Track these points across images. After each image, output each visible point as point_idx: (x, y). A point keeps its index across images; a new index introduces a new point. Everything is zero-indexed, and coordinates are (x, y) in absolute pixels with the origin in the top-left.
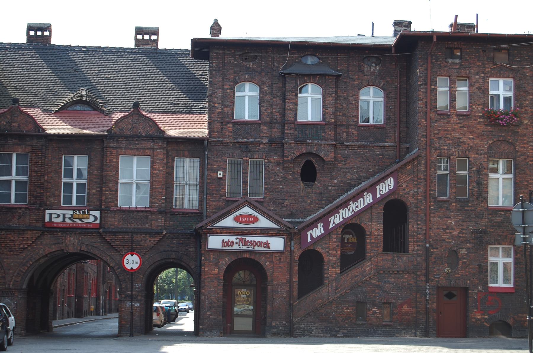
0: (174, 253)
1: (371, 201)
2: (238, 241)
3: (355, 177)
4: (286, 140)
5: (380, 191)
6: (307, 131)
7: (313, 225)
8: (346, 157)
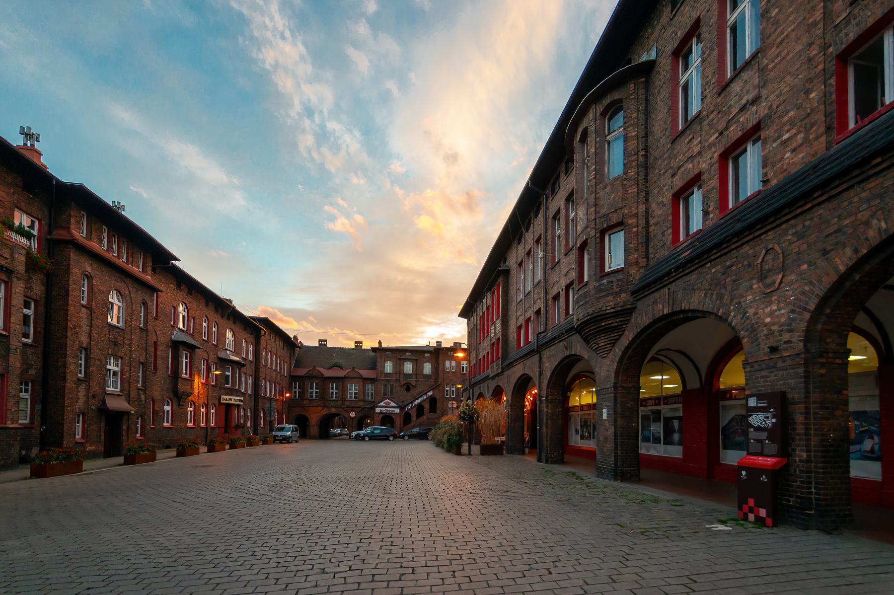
7: (408, 405)
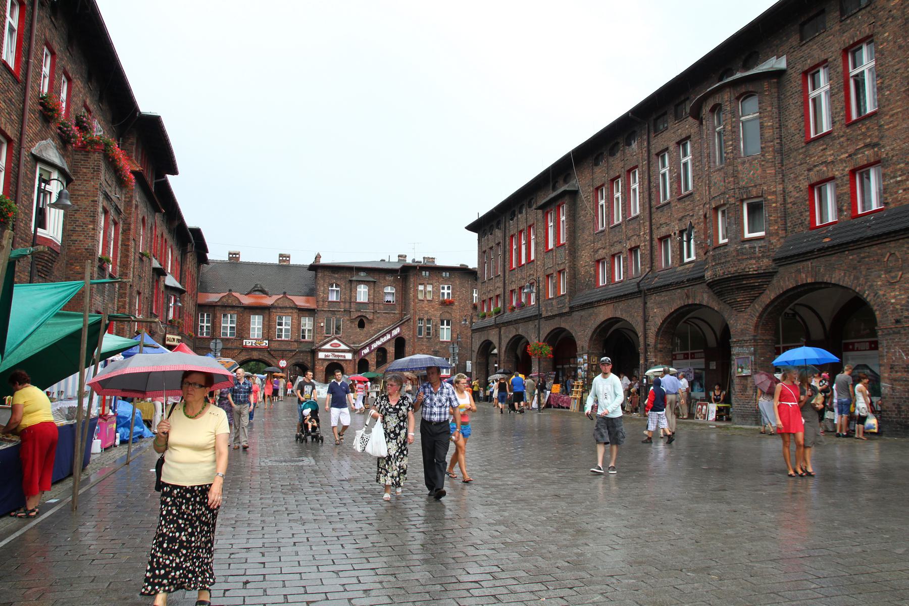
7: (364, 348)
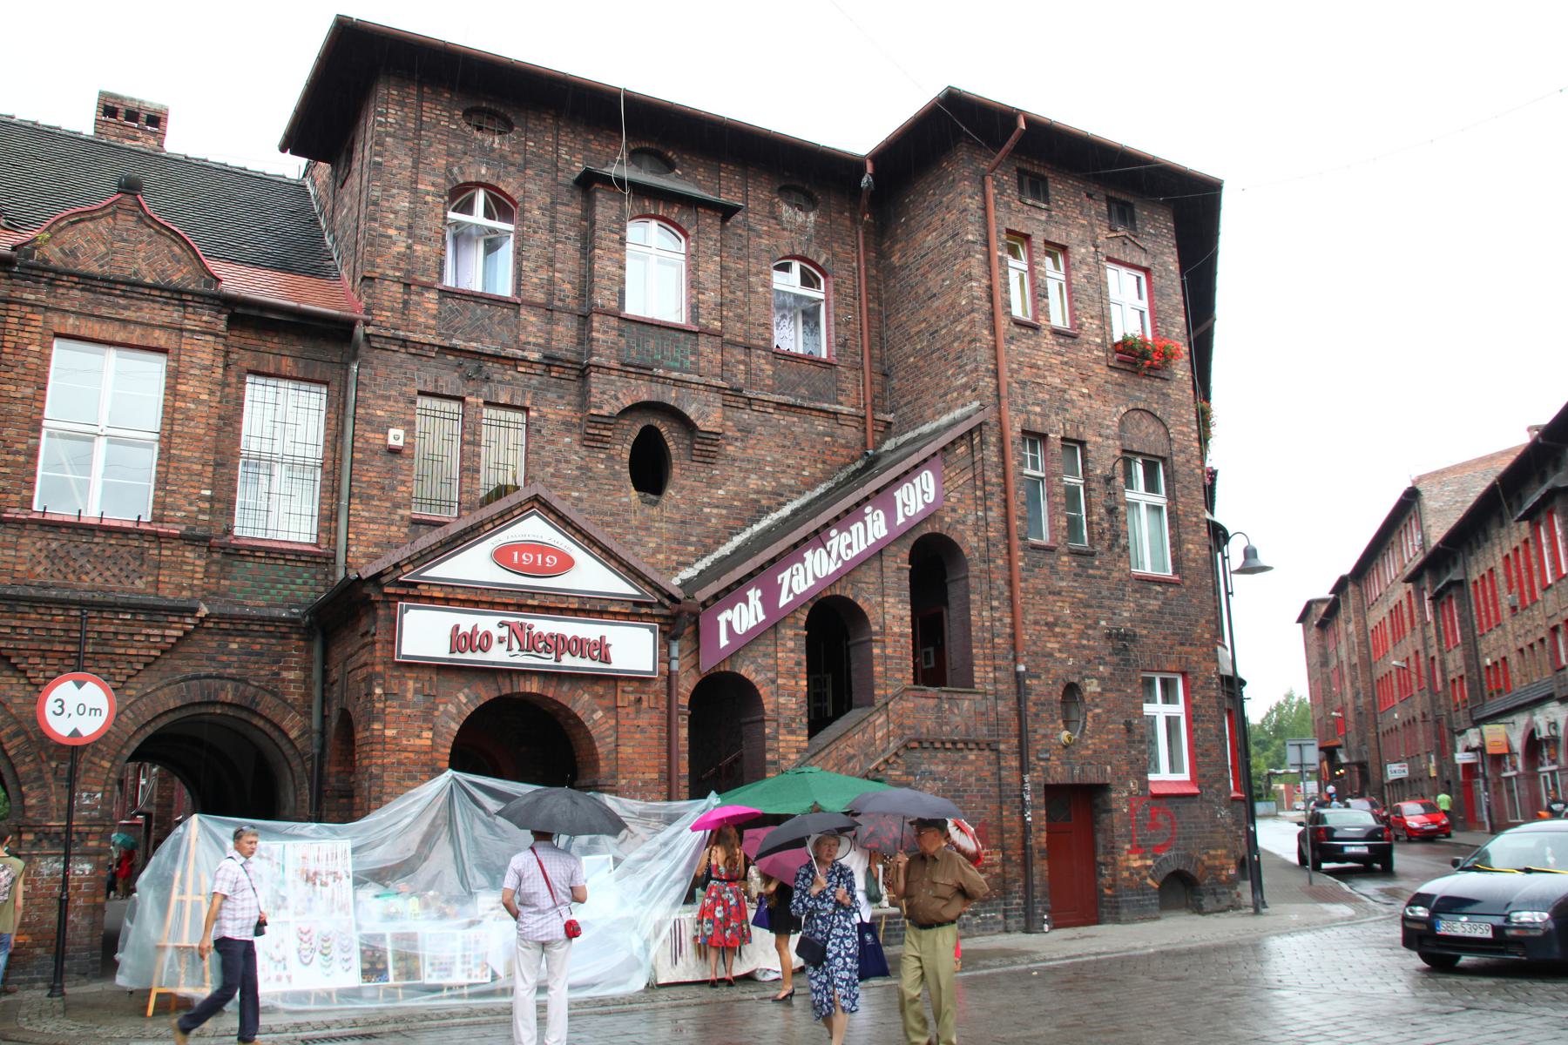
0: (229, 686)
1: (884, 532)
2: (505, 632)
3: (769, 485)
4: (595, 359)
5: (905, 505)
6: (651, 345)
7: (732, 594)
8: (746, 431)
